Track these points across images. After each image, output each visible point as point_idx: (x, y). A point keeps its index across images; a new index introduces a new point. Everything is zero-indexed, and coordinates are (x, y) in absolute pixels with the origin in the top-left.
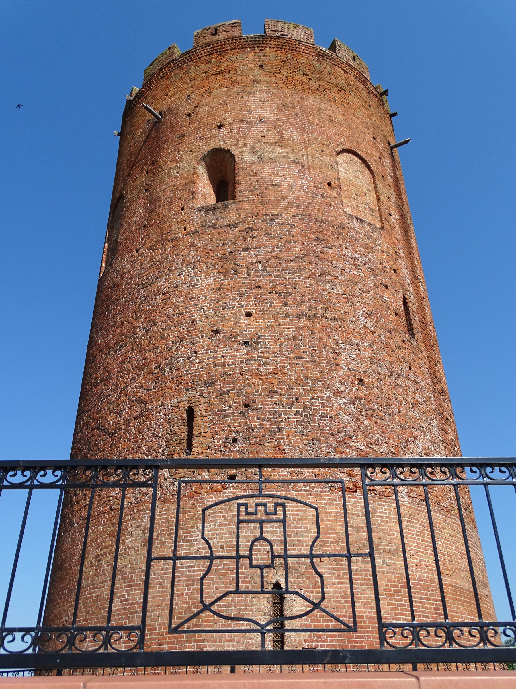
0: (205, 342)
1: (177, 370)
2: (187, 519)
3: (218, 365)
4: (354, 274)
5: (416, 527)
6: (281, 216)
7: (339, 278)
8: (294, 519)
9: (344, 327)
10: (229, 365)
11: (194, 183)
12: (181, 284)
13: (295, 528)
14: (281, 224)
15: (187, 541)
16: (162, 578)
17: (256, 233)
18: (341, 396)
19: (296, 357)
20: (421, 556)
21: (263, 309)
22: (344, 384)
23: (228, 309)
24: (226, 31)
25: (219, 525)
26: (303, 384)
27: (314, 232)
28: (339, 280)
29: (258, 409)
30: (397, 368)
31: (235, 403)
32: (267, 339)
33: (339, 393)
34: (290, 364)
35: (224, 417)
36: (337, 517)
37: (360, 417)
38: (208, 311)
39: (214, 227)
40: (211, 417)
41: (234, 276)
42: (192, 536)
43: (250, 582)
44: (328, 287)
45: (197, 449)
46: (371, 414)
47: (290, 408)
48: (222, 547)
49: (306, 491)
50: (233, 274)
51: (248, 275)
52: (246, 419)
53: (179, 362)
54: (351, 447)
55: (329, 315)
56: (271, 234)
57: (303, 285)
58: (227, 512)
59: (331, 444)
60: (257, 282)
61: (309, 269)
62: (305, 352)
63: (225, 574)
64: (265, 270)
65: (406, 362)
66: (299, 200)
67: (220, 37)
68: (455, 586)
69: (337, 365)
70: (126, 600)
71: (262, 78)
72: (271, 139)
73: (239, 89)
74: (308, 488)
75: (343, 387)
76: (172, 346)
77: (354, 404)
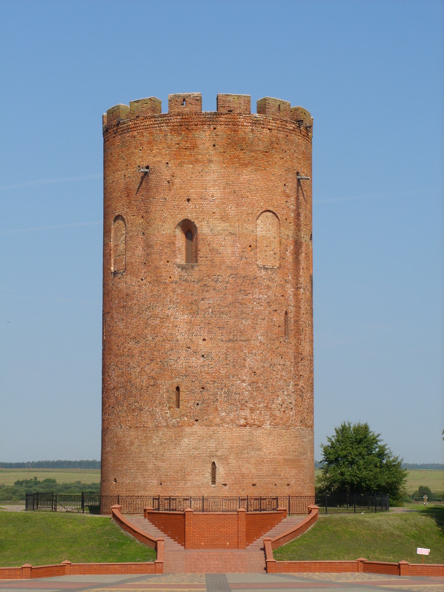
0: (184, 353)
1: (171, 366)
2: (178, 436)
3: (190, 367)
4: (258, 309)
5: (271, 438)
6: (222, 276)
7: (250, 314)
8: (221, 438)
9: (250, 344)
10: (195, 367)
11: (174, 244)
12: (170, 315)
13: (221, 442)
14: (222, 282)
15: (179, 445)
16: (170, 458)
17: (209, 288)
18: (244, 382)
19: (226, 364)
20: (272, 449)
21: (211, 337)
22: (246, 376)
23: (195, 335)
24: (191, 104)
25: (192, 440)
26: (227, 377)
27: (239, 285)
28: (250, 316)
29: (208, 390)
30: (275, 361)
31: (198, 386)
32: (213, 354)
33: (243, 381)
34: (222, 367)
35: (193, 393)
36: (237, 437)
37: (252, 391)
38: (185, 335)
39: (186, 281)
40: (187, 393)
41: (197, 316)
42: (181, 443)
43: (204, 462)
44: (244, 321)
45: (182, 407)
46: (258, 389)
47: (222, 390)
48: (193, 448)
49: (226, 427)
50: (196, 315)
51: (204, 316)
52: (202, 395)
53: (172, 361)
54: (247, 406)
55: (243, 338)
56: (216, 289)
57: (232, 321)
58: (195, 435)
59: (238, 406)
60: (209, 321)
61: (235, 312)
62: (230, 361)
63: (194, 458)
64: (213, 313)
65: (280, 355)
66: (232, 263)
67: (186, 109)
68: (285, 459)
69: (244, 366)
70: (155, 464)
71: (214, 159)
72: (218, 215)
73: (199, 167)
74: (227, 426)
75: (246, 378)
76: (167, 352)
77: (250, 386)
